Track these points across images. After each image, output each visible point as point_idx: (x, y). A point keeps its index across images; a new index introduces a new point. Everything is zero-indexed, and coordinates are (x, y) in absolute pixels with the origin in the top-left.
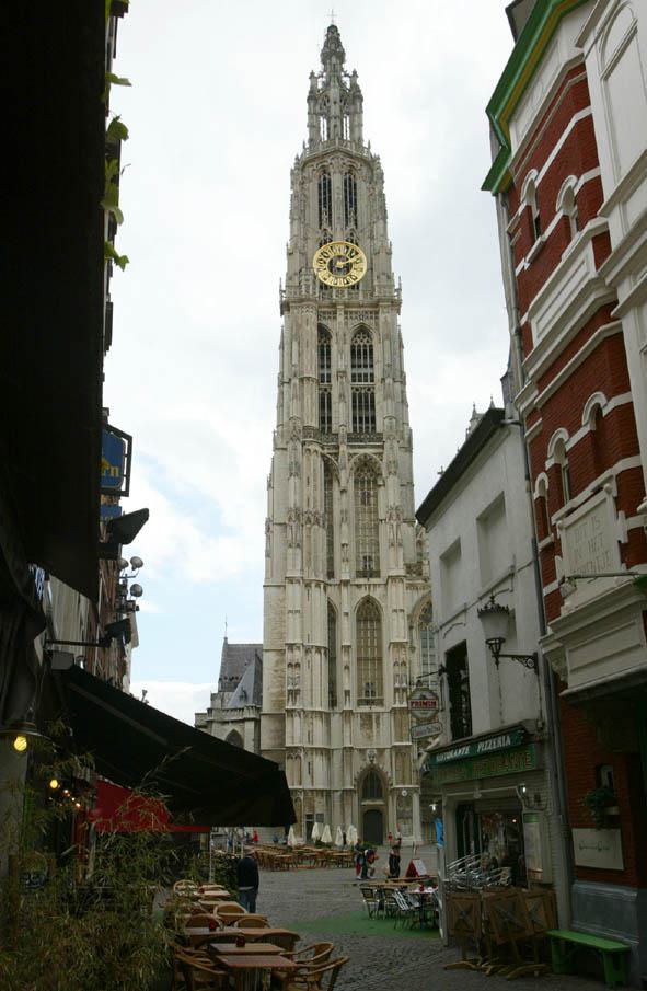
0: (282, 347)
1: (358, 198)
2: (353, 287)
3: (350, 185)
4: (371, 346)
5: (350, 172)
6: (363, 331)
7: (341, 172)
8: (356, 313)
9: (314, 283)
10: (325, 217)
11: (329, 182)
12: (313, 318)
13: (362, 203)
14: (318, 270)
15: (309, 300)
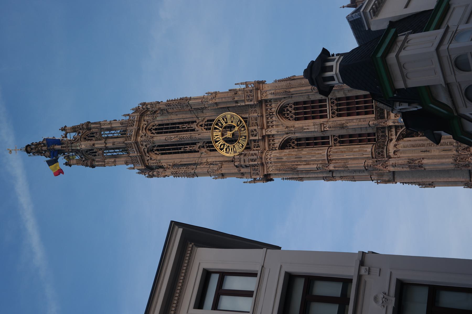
0: (301, 179)
1: (171, 122)
2: (246, 122)
3: (159, 129)
4: (296, 103)
5: (150, 130)
6: (282, 112)
7: (153, 137)
8: (267, 118)
9: (245, 155)
10: (188, 148)
11: (159, 146)
12: (275, 154)
13: (175, 118)
14: (235, 152)
15: (261, 158)
